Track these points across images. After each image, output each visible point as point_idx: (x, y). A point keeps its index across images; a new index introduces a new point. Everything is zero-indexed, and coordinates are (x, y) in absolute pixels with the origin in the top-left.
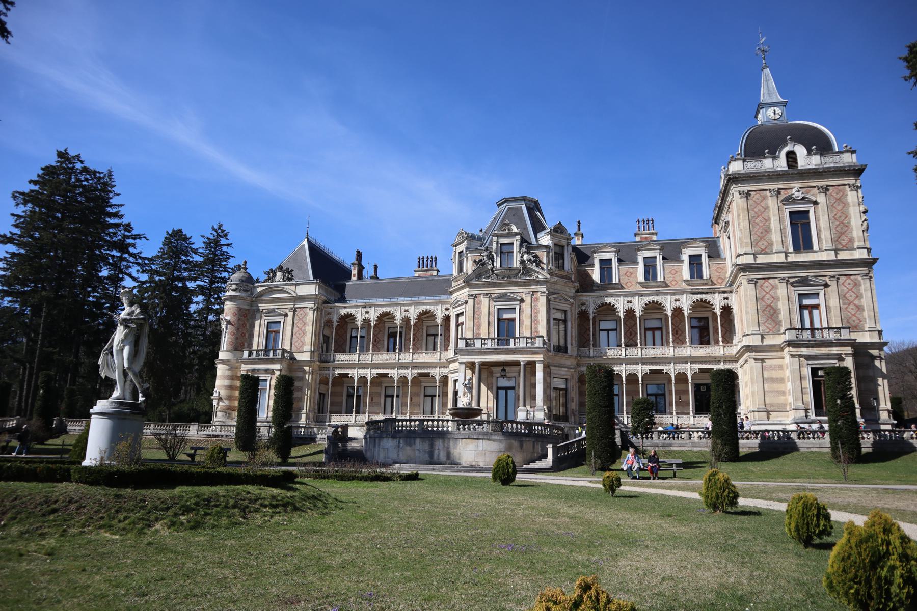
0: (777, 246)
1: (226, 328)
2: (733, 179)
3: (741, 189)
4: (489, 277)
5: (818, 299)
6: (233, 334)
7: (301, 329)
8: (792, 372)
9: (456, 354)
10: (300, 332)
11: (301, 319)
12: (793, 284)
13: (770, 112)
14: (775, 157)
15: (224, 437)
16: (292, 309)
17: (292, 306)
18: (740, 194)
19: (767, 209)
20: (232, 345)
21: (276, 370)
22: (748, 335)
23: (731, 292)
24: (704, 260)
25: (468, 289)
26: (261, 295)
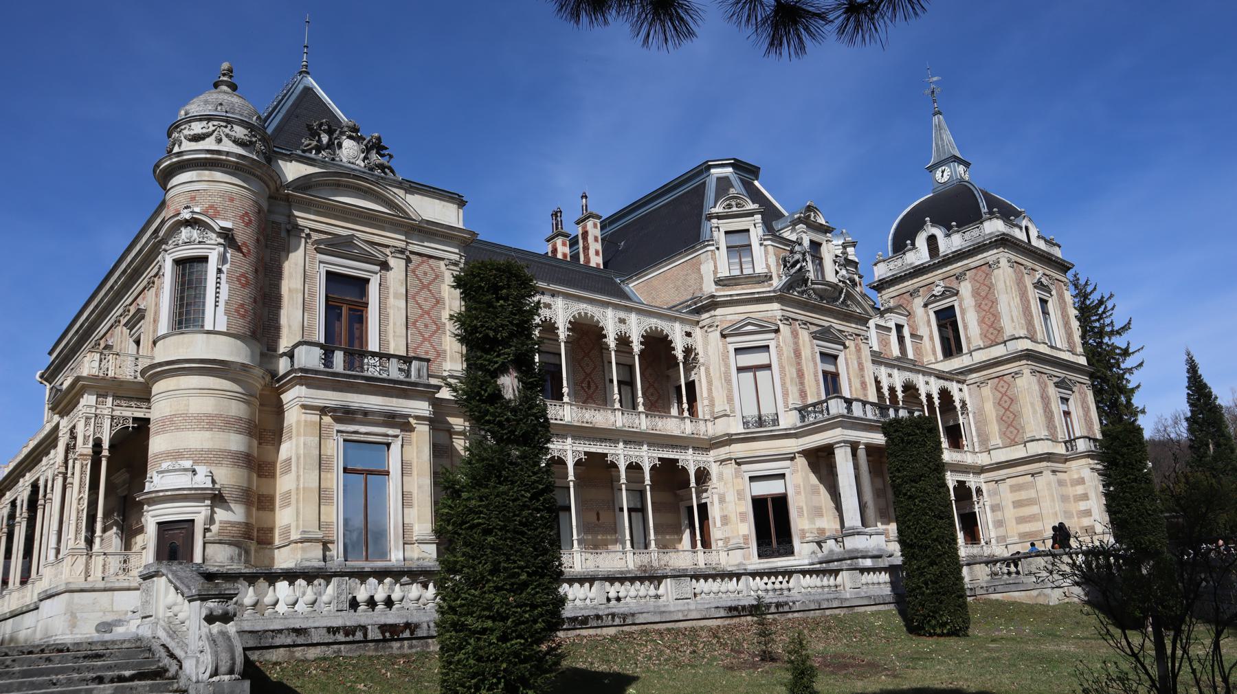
0: (1039, 337)
1: (223, 259)
2: (1003, 241)
3: (1011, 256)
4: (802, 293)
5: (1068, 405)
6: (240, 280)
7: (428, 314)
8: (1096, 487)
9: (746, 424)
10: (427, 319)
11: (424, 287)
12: (1057, 385)
13: (961, 169)
14: (1021, 228)
15: (773, 609)
16: (402, 251)
17: (403, 245)
18: (1009, 261)
19: (1026, 287)
20: (243, 316)
21: (417, 418)
22: (1042, 439)
23: (963, 383)
24: (906, 332)
25: (776, 306)
26: (304, 184)
